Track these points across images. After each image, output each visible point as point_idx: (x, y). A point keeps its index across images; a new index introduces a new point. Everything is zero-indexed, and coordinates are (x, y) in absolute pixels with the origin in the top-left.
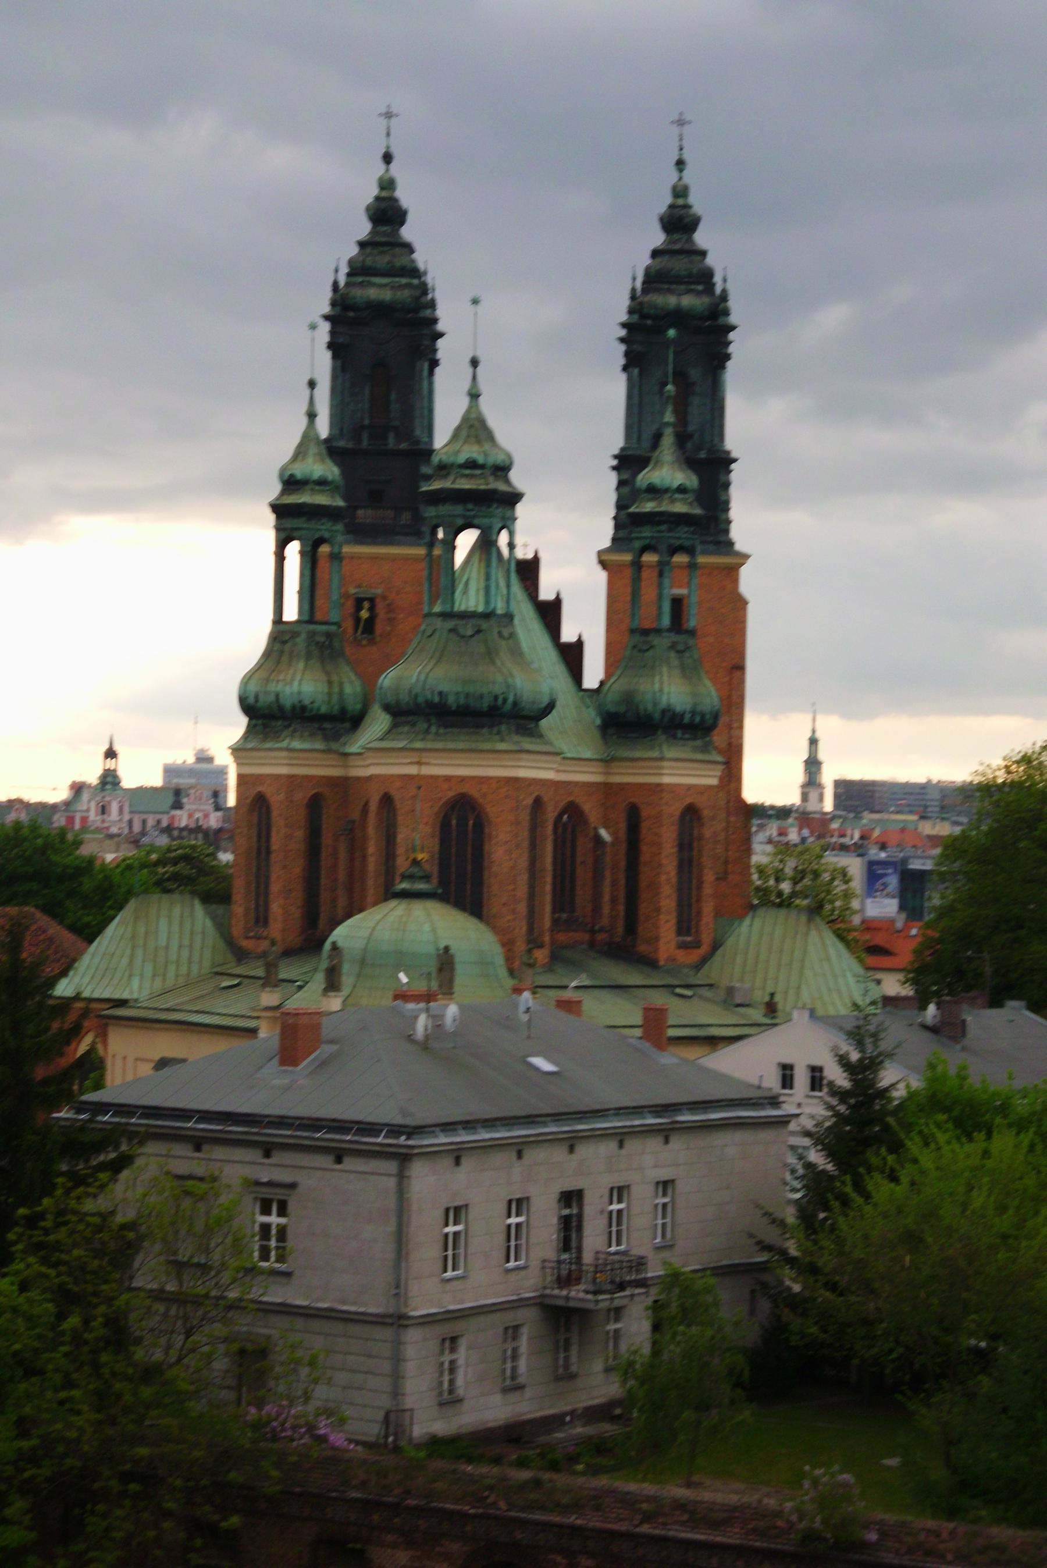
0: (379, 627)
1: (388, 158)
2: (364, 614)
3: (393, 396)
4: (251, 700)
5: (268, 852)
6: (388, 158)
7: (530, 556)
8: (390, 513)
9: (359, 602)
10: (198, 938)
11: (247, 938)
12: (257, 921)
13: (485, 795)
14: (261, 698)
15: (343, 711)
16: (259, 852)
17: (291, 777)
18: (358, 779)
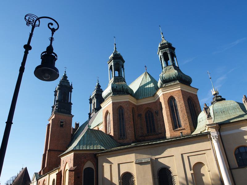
0: (64, 126)
1: (65, 72)
2: (62, 124)
3: (66, 97)
4: (115, 88)
5: (123, 119)
6: (65, 72)
7: (78, 123)
8: (66, 111)
9: (61, 122)
10: (108, 139)
11: (119, 139)
12: (121, 135)
13: (193, 97)
14: (118, 87)
15: (132, 93)
16: (120, 119)
17: (129, 101)
18: (141, 105)
